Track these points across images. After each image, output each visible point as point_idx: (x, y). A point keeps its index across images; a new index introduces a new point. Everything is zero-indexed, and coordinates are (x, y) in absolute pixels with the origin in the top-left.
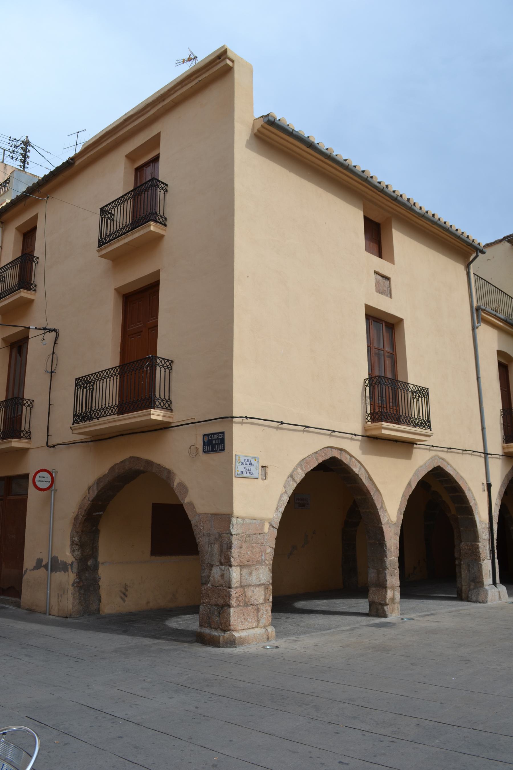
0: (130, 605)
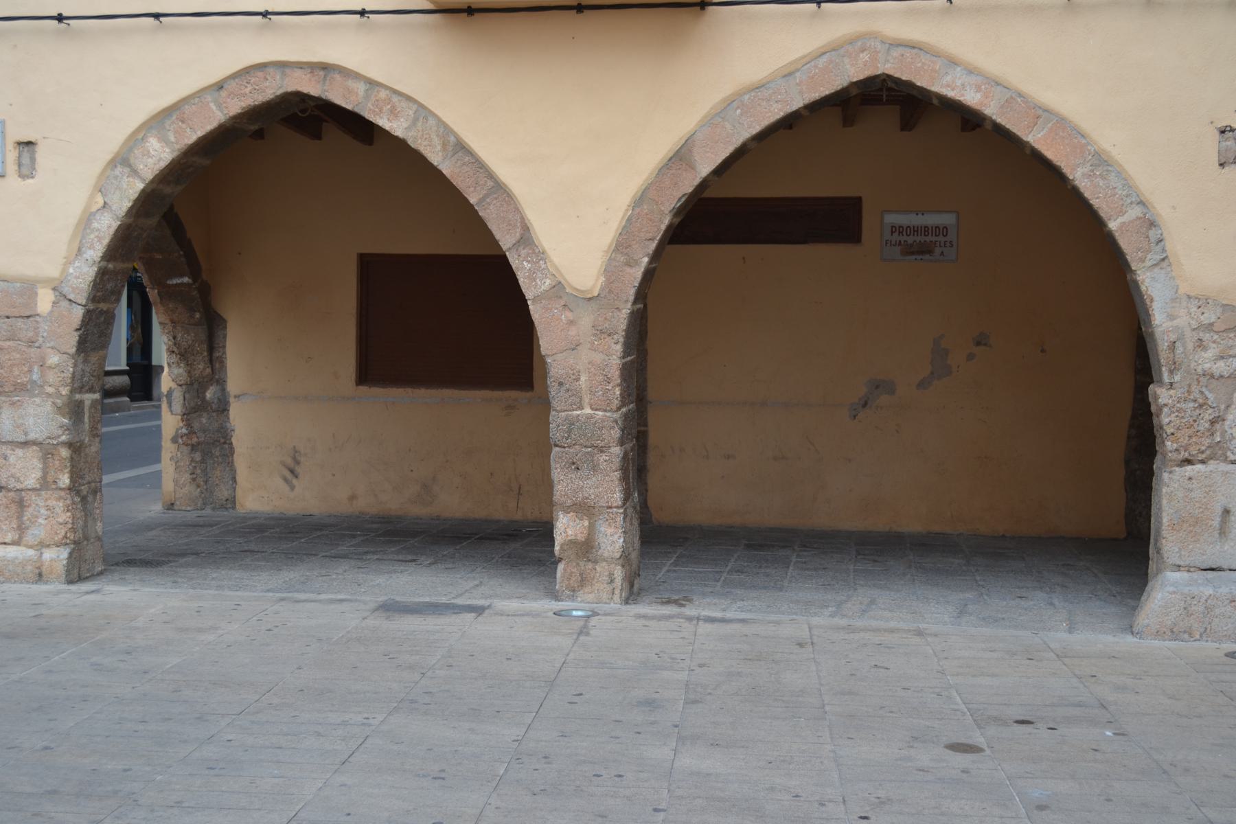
0: (305, 499)
